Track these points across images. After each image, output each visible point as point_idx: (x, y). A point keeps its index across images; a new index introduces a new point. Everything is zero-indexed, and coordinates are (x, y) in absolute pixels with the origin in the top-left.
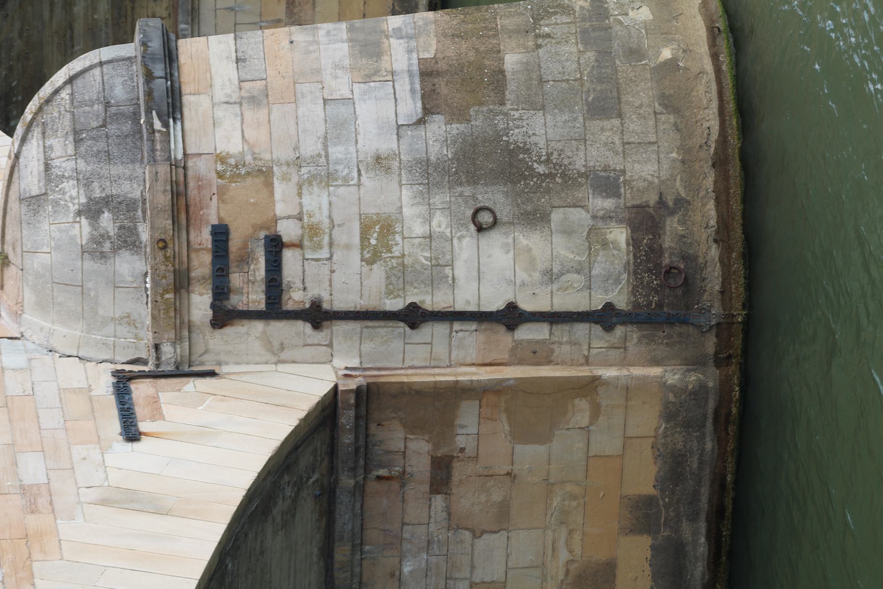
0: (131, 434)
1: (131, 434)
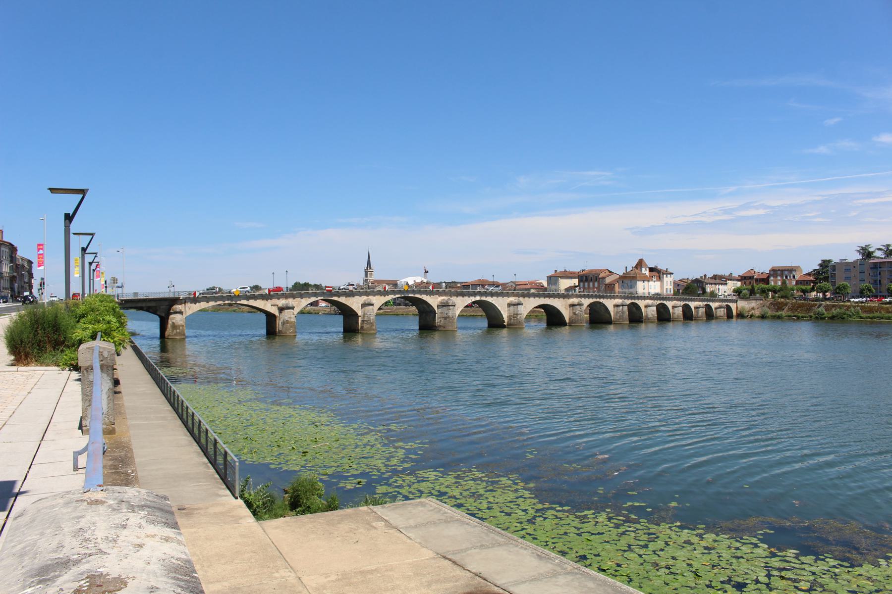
0: (272, 305)
1: (272, 305)
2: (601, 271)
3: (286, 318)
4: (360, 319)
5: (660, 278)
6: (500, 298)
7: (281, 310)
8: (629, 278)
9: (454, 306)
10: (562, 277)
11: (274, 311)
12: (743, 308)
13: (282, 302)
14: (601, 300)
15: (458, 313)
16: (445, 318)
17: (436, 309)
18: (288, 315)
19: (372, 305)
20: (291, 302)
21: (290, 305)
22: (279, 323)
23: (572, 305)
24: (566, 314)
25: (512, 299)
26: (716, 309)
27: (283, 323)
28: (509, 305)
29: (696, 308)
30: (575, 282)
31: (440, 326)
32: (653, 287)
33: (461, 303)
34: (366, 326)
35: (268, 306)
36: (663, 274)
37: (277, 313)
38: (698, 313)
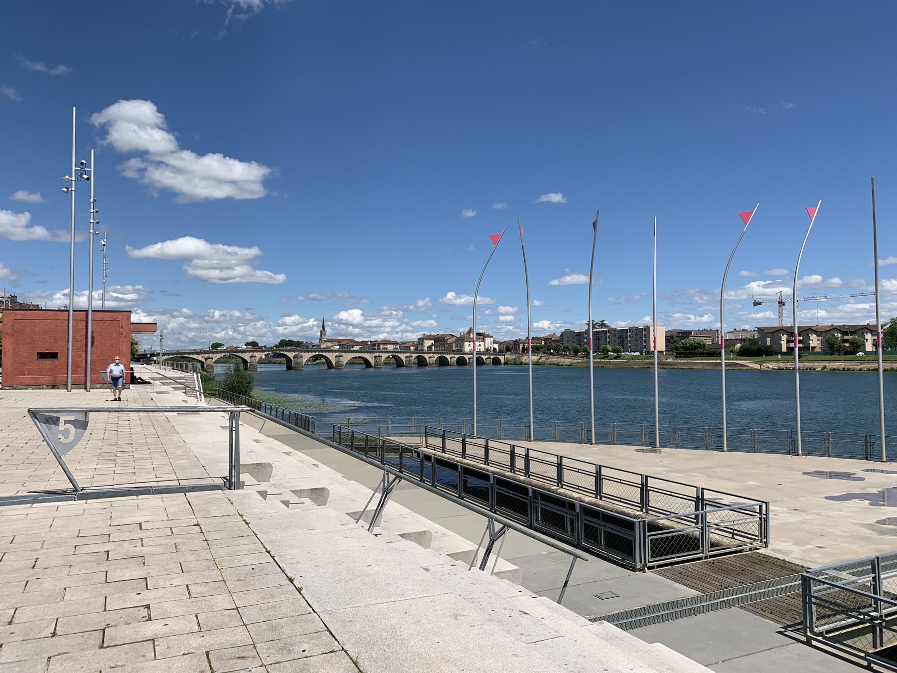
2: (447, 335)
3: (208, 363)
4: (249, 364)
5: (484, 340)
6: (331, 353)
7: (206, 359)
8: (461, 340)
9: (302, 357)
10: (426, 339)
11: (203, 360)
12: (507, 358)
13: (206, 356)
14: (397, 354)
15: (304, 361)
16: (296, 363)
17: (292, 359)
18: (209, 361)
19: (255, 357)
20: (211, 355)
21: (210, 357)
22: (205, 365)
23: (375, 357)
24: (372, 362)
25: (337, 354)
26: (486, 359)
27: (207, 365)
28: (336, 357)
29: (469, 359)
30: (433, 342)
31: (294, 367)
32: (480, 346)
33: (306, 356)
34: (251, 367)
35: (200, 357)
36: (486, 337)
37: (204, 361)
38: (469, 361)
